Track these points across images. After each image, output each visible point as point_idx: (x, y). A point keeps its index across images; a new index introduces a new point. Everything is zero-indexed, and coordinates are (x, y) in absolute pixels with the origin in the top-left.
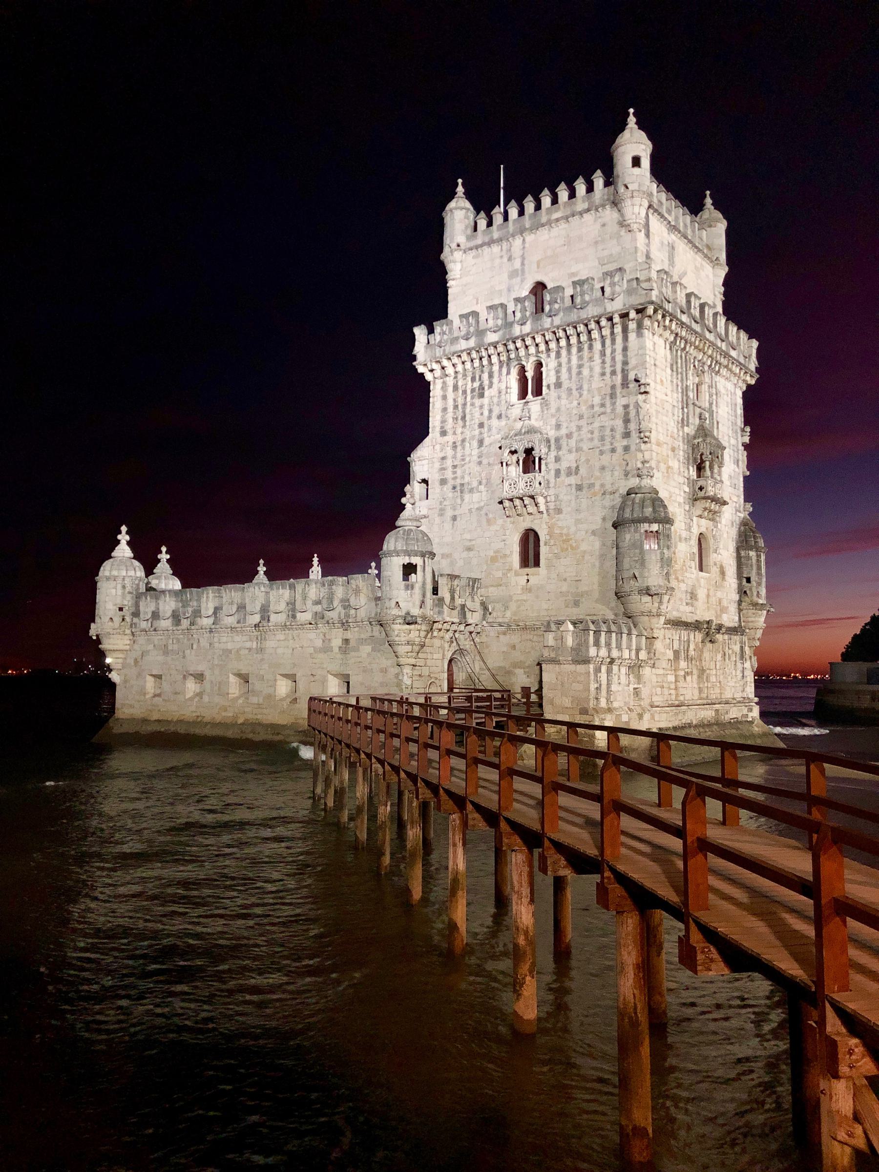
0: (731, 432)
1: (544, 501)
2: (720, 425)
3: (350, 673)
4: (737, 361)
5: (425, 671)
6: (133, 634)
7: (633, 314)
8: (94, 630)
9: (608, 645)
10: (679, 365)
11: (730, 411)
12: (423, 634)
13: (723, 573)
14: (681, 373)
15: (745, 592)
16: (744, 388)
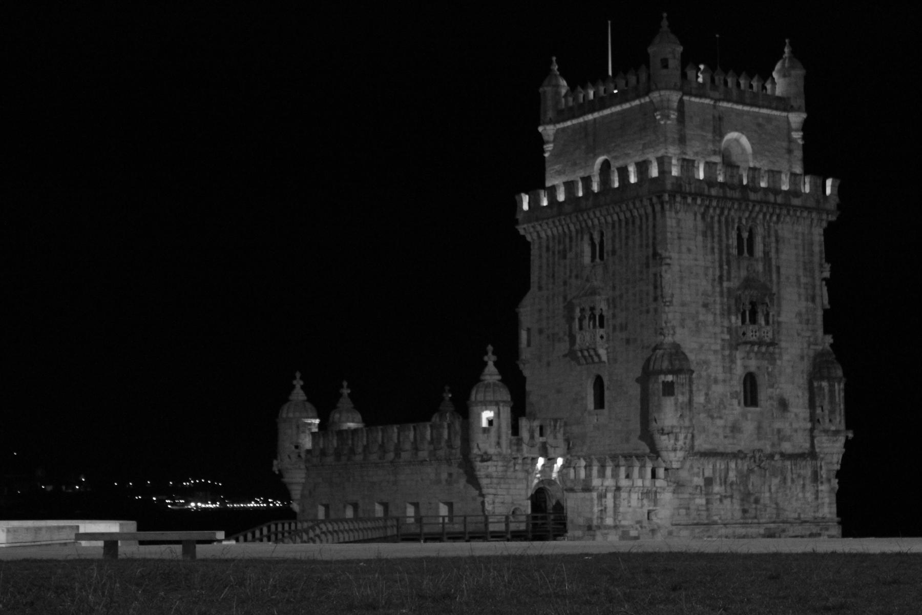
0: (801, 273)
1: (605, 352)
2: (783, 271)
3: (453, 501)
5: (508, 499)
6: (307, 468)
7: (655, 200)
8: (276, 466)
9: (615, 476)
10: (716, 229)
11: (801, 253)
12: (500, 469)
13: (783, 405)
14: (720, 236)
15: (818, 420)
16: (825, 224)
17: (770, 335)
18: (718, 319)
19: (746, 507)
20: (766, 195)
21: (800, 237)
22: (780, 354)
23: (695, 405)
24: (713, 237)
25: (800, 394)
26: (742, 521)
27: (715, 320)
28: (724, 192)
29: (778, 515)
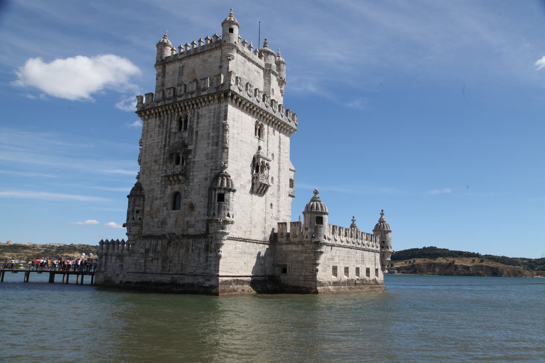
0: (211, 131)
4: (205, 96)
10: (165, 122)
11: (212, 120)
13: (192, 207)
14: (167, 125)
17: (179, 170)
18: (161, 167)
19: (165, 265)
20: (186, 96)
21: (213, 111)
22: (193, 179)
23: (145, 212)
24: (163, 126)
25: (203, 200)
26: (159, 272)
27: (159, 167)
28: (165, 103)
29: (182, 270)
